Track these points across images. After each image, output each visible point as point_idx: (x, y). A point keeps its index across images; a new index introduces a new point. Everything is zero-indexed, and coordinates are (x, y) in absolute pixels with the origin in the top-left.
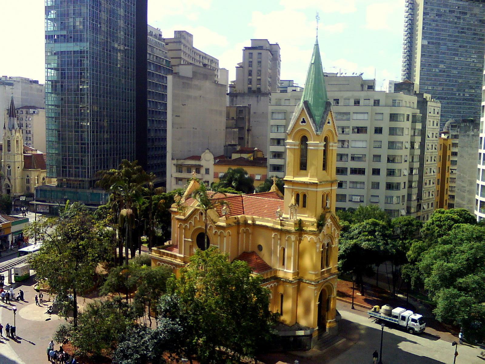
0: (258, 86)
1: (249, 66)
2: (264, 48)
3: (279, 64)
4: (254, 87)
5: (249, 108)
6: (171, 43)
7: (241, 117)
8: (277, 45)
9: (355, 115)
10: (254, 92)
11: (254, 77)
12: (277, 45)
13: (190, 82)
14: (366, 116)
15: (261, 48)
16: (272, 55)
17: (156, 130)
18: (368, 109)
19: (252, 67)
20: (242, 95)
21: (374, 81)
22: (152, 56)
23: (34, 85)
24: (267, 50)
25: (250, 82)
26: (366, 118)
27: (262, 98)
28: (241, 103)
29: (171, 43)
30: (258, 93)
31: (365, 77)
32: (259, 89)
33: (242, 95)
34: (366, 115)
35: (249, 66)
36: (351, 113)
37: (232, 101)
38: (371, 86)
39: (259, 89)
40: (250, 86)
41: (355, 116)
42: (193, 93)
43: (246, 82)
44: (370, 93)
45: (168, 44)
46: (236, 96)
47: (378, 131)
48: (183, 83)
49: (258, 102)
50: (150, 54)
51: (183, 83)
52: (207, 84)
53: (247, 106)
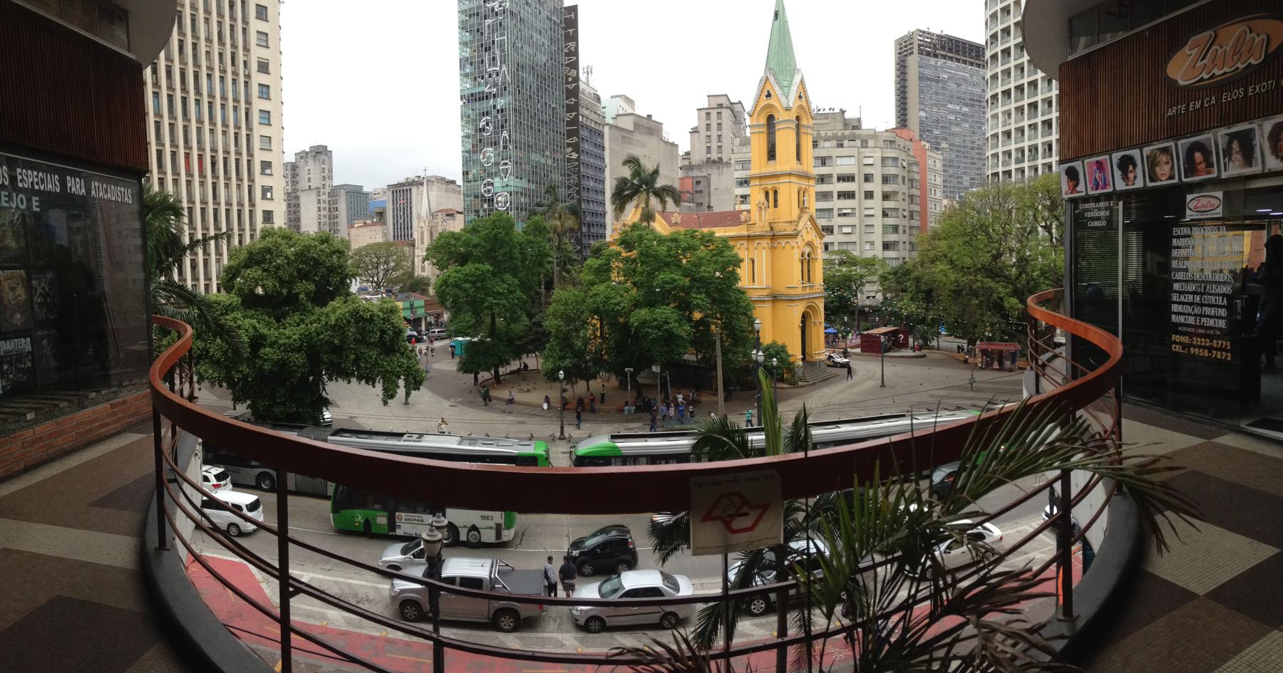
0: (719, 155)
2: (725, 106)
4: (714, 156)
5: (708, 178)
8: (740, 103)
9: (838, 159)
10: (714, 162)
11: (714, 145)
12: (740, 103)
14: (852, 161)
15: (720, 106)
18: (854, 151)
21: (859, 120)
24: (726, 108)
25: (709, 148)
26: (853, 163)
27: (725, 169)
28: (696, 173)
30: (719, 162)
31: (847, 116)
32: (720, 159)
33: (699, 167)
34: (853, 158)
36: (834, 157)
38: (856, 125)
40: (709, 156)
41: (839, 161)
43: (704, 149)
44: (857, 132)
46: (692, 170)
47: (868, 178)
50: (583, 116)
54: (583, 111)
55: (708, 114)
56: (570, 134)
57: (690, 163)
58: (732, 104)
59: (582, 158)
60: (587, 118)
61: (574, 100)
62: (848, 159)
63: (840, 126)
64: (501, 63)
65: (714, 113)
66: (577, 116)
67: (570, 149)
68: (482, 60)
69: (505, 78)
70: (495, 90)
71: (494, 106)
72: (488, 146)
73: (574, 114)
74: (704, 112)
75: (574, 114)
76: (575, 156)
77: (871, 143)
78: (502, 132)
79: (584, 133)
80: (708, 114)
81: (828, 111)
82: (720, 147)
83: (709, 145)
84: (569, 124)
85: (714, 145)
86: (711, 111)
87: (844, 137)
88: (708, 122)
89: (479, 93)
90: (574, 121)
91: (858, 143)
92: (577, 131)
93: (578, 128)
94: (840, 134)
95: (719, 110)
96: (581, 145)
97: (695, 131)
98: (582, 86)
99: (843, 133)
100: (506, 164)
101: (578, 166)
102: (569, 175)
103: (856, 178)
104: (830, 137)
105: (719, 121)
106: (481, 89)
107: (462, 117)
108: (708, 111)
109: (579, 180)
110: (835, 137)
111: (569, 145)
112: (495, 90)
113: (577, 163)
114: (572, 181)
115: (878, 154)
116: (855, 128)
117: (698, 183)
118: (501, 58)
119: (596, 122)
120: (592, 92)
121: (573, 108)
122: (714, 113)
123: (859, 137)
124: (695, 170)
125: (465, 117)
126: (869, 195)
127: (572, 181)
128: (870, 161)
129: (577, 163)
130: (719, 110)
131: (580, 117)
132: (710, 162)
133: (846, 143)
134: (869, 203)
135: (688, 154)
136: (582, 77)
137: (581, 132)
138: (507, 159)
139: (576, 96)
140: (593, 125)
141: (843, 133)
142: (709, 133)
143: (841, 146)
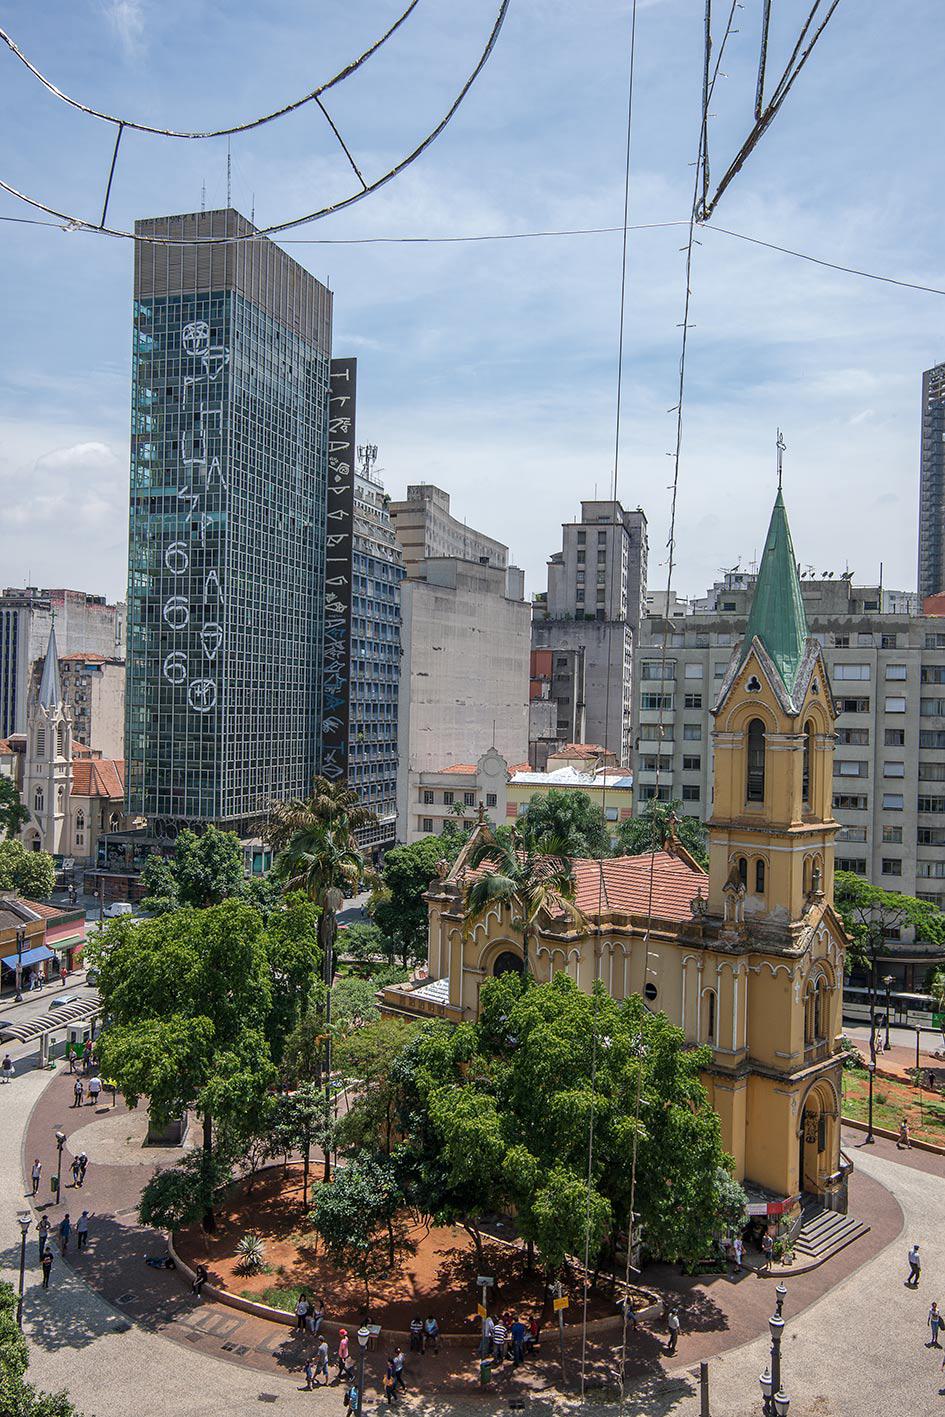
0: (600, 605)
1: (579, 561)
3: (645, 556)
4: (591, 606)
6: (401, 511)
7: (562, 673)
8: (640, 512)
9: (838, 669)
10: (590, 618)
11: (591, 589)
13: (451, 597)
14: (866, 672)
16: (630, 537)
17: (368, 705)
19: (584, 562)
20: (564, 623)
22: (361, 542)
23: (95, 609)
25: (580, 596)
29: (401, 511)
30: (597, 620)
31: (856, 583)
32: (601, 612)
34: (866, 669)
35: (579, 561)
37: (538, 639)
38: (871, 599)
39: (601, 612)
40: (580, 605)
42: (456, 621)
43: (572, 593)
45: (395, 516)
46: (550, 629)
48: (436, 598)
49: (599, 638)
50: (357, 537)
51: (436, 598)
52: (489, 604)
53: (577, 649)
54: (359, 529)
55: (582, 534)
56: (333, 570)
57: (547, 615)
58: (625, 513)
59: (353, 610)
60: (366, 540)
61: (342, 512)
62: (858, 668)
63: (844, 606)
64: (210, 453)
65: (592, 533)
66: (348, 541)
67: (333, 596)
68: (175, 444)
69: (217, 481)
70: (196, 497)
71: (195, 527)
72: (179, 593)
73: (342, 536)
74: (575, 531)
75: (342, 536)
76: (340, 608)
77: (902, 639)
78: (207, 574)
79: (359, 569)
80: (582, 534)
81: (821, 579)
82: (601, 591)
83: (581, 586)
84: (331, 553)
85: (591, 589)
86: (588, 529)
87: (849, 627)
88: (581, 547)
89: (167, 498)
90: (345, 548)
91: (878, 637)
92: (348, 565)
93: (350, 560)
94: (842, 621)
95: (601, 528)
96: (354, 587)
97: (558, 560)
98: (358, 483)
99: (850, 620)
100: (213, 629)
101: (347, 626)
102: (328, 641)
103: (872, 704)
104: (823, 626)
105: (602, 547)
106: (170, 492)
107: (131, 535)
108: (582, 529)
109: (347, 650)
110: (832, 626)
111: (330, 588)
112: (196, 497)
113: (344, 621)
114: (332, 651)
115: (915, 661)
116: (871, 606)
117: (563, 662)
118: (210, 442)
119: (380, 546)
120: (374, 491)
121: (346, 526)
122: (592, 533)
123: (880, 627)
124: (554, 631)
125: (136, 536)
126: (897, 737)
127: (332, 651)
128: (900, 673)
129: (344, 621)
130: (601, 528)
131: (354, 539)
132: (581, 618)
133: (853, 637)
134: (895, 753)
135: (543, 597)
136: (359, 467)
137: (355, 566)
138: (214, 620)
139: (350, 509)
140: (376, 553)
141: (850, 620)
142: (581, 566)
143: (842, 643)
